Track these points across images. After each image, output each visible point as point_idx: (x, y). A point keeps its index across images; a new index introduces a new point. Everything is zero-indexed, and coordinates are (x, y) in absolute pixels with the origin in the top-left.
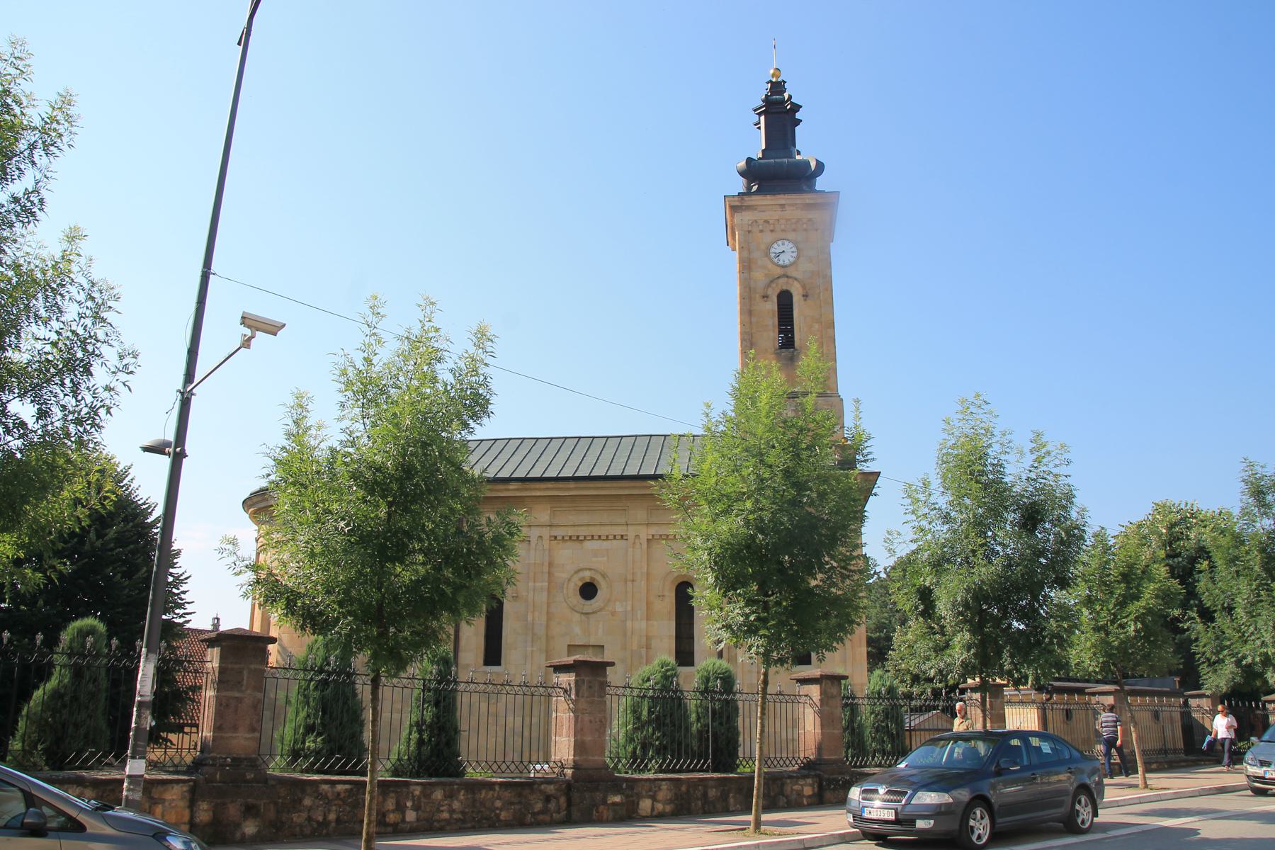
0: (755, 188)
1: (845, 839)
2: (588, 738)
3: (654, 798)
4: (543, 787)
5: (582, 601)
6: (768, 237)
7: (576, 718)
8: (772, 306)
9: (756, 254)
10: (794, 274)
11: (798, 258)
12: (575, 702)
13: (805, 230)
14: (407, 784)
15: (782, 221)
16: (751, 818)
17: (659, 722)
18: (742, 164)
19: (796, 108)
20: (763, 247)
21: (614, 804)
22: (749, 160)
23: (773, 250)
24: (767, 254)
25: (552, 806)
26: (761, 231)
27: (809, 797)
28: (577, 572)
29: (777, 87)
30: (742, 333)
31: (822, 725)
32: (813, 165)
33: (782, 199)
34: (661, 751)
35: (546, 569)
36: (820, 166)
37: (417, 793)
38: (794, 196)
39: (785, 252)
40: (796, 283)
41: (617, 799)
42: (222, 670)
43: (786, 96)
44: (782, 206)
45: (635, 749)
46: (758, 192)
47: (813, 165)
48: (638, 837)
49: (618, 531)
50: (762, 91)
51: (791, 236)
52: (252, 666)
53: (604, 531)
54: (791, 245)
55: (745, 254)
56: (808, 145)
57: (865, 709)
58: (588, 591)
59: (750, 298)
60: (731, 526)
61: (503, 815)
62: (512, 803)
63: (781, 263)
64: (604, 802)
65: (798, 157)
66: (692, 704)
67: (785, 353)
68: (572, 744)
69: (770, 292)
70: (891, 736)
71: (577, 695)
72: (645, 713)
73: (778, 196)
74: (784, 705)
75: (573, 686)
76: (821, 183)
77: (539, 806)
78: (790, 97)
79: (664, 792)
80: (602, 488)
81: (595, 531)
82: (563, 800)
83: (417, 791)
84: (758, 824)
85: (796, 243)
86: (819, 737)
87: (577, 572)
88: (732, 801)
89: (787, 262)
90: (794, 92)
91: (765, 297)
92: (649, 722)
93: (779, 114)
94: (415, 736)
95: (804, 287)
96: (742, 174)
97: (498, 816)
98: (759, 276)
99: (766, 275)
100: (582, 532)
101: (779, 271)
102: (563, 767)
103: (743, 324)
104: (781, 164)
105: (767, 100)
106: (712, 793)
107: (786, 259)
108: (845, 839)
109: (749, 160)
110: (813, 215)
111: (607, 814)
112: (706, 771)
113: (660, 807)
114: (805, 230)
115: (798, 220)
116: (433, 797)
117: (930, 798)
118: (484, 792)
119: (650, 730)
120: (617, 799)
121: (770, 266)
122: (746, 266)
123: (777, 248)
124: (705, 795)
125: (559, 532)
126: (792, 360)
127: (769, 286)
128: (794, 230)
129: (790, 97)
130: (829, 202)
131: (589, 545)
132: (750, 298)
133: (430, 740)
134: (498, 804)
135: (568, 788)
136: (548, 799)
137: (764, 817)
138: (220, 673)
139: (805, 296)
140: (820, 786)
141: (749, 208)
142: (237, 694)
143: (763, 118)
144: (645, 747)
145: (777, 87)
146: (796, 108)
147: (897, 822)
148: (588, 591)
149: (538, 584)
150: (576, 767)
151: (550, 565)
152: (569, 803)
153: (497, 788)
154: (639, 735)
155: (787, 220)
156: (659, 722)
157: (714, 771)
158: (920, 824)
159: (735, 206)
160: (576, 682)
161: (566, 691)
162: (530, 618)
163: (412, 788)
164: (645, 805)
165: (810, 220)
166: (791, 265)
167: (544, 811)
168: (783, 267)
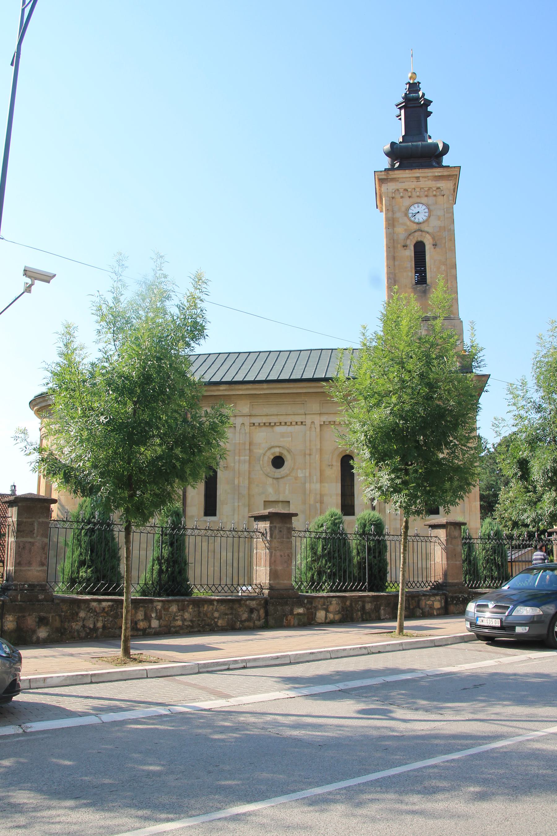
0: (397, 165)
1: (464, 640)
2: (279, 568)
3: (327, 610)
4: (248, 602)
5: (274, 469)
6: (406, 202)
7: (271, 553)
8: (410, 253)
9: (398, 215)
10: (426, 229)
11: (429, 216)
12: (270, 542)
13: (435, 196)
14: (151, 601)
15: (418, 190)
16: (396, 624)
17: (330, 556)
18: (387, 147)
19: (428, 103)
20: (403, 209)
21: (299, 614)
22: (393, 144)
23: (410, 211)
24: (406, 215)
25: (254, 616)
26: (402, 197)
27: (438, 609)
28: (270, 448)
29: (414, 87)
30: (388, 273)
31: (447, 558)
32: (441, 147)
33: (417, 173)
34: (332, 576)
35: (247, 447)
36: (446, 148)
37: (159, 607)
38: (426, 170)
39: (420, 212)
41: (301, 611)
42: (19, 523)
43: (420, 94)
44: (418, 178)
45: (313, 575)
46: (399, 168)
47: (441, 147)
48: (316, 637)
49: (299, 419)
50: (403, 90)
51: (424, 200)
52: (41, 520)
53: (289, 419)
54: (424, 207)
55: (390, 214)
56: (436, 132)
57: (478, 546)
58: (278, 462)
59: (394, 247)
60: (380, 415)
61: (220, 623)
62: (226, 614)
63: (417, 221)
64: (291, 612)
65: (430, 141)
66: (353, 543)
67: (420, 287)
68: (268, 572)
69: (408, 242)
70: (497, 566)
71: (271, 536)
72: (320, 549)
74: (419, 543)
75: (268, 530)
76: (446, 160)
77: (245, 616)
78: (423, 95)
79: (334, 606)
80: (287, 388)
81: (283, 419)
82: (262, 612)
83: (159, 606)
84: (401, 628)
85: (428, 206)
86: (445, 566)
87: (270, 448)
88: (382, 612)
89: (421, 220)
90: (426, 91)
91: (405, 246)
92: (323, 556)
93: (415, 108)
94: (156, 567)
95: (433, 238)
96: (388, 154)
97: (216, 623)
98: (400, 231)
99: (406, 230)
100: (273, 420)
101: (415, 227)
102: (262, 588)
103: (388, 267)
104: (417, 146)
105: (406, 98)
106: (368, 606)
107: (421, 218)
108: (464, 640)
109: (393, 144)
111: (294, 621)
112: (364, 591)
113: (331, 616)
114: (435, 196)
115: (429, 189)
116: (170, 610)
117: (526, 611)
118: (206, 607)
119: (324, 562)
120: (301, 611)
121: (408, 223)
122: (391, 223)
123: (413, 210)
124: (363, 607)
125: (256, 420)
126: (425, 293)
127: (408, 238)
128: (427, 196)
129: (423, 95)
131: (278, 429)
132: (394, 247)
133: (167, 570)
134: (216, 614)
135: (266, 603)
136: (251, 611)
137: (406, 624)
138: (18, 525)
139: (435, 245)
140: (446, 602)
141: (393, 180)
142: (30, 540)
143: (403, 111)
144: (320, 574)
145: (414, 87)
146: (428, 103)
147: (502, 628)
148: (278, 462)
149: (242, 458)
150: (271, 588)
151: (250, 444)
152: (267, 614)
153: (215, 603)
154: (316, 565)
156: (330, 556)
157: (369, 591)
158: (519, 630)
159: (383, 179)
160: (271, 528)
161: (263, 534)
162: (236, 482)
163: (155, 604)
164: (321, 615)
165: (438, 188)
167: (249, 619)
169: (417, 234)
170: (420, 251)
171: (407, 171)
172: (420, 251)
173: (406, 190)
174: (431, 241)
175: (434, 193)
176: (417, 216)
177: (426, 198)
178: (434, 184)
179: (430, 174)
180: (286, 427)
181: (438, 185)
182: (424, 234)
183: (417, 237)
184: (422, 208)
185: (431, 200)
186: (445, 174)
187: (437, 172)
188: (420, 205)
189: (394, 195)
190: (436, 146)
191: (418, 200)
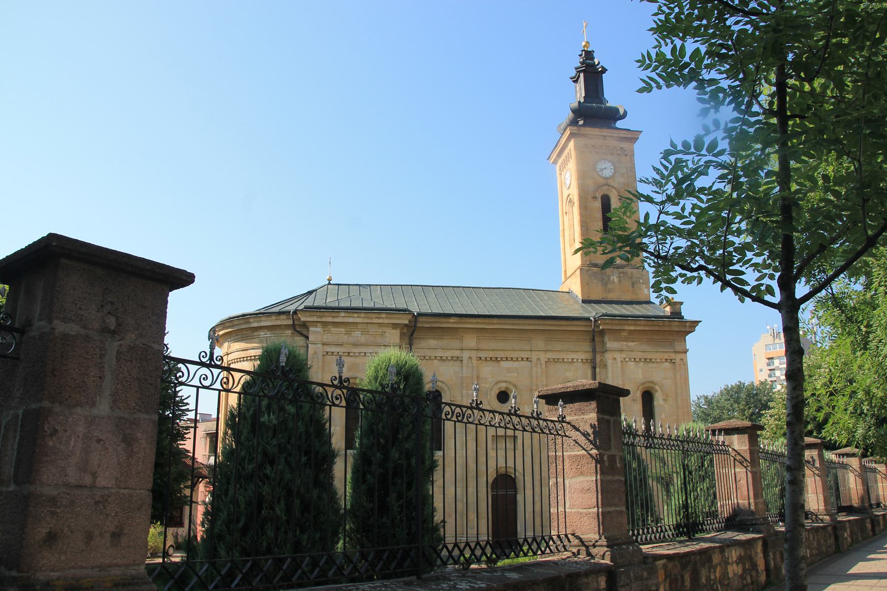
10: (613, 184)
11: (615, 173)
13: (619, 155)
32: (622, 112)
39: (607, 169)
81: (509, 354)
89: (608, 175)
91: (595, 198)
100: (500, 354)
101: (603, 181)
107: (608, 173)
114: (619, 155)
125: (483, 355)
128: (612, 154)
131: (504, 364)
168: (606, 178)
169: (605, 188)
176: (604, 171)
178: (615, 143)
181: (622, 146)
183: (604, 190)
184: (608, 165)
190: (617, 110)
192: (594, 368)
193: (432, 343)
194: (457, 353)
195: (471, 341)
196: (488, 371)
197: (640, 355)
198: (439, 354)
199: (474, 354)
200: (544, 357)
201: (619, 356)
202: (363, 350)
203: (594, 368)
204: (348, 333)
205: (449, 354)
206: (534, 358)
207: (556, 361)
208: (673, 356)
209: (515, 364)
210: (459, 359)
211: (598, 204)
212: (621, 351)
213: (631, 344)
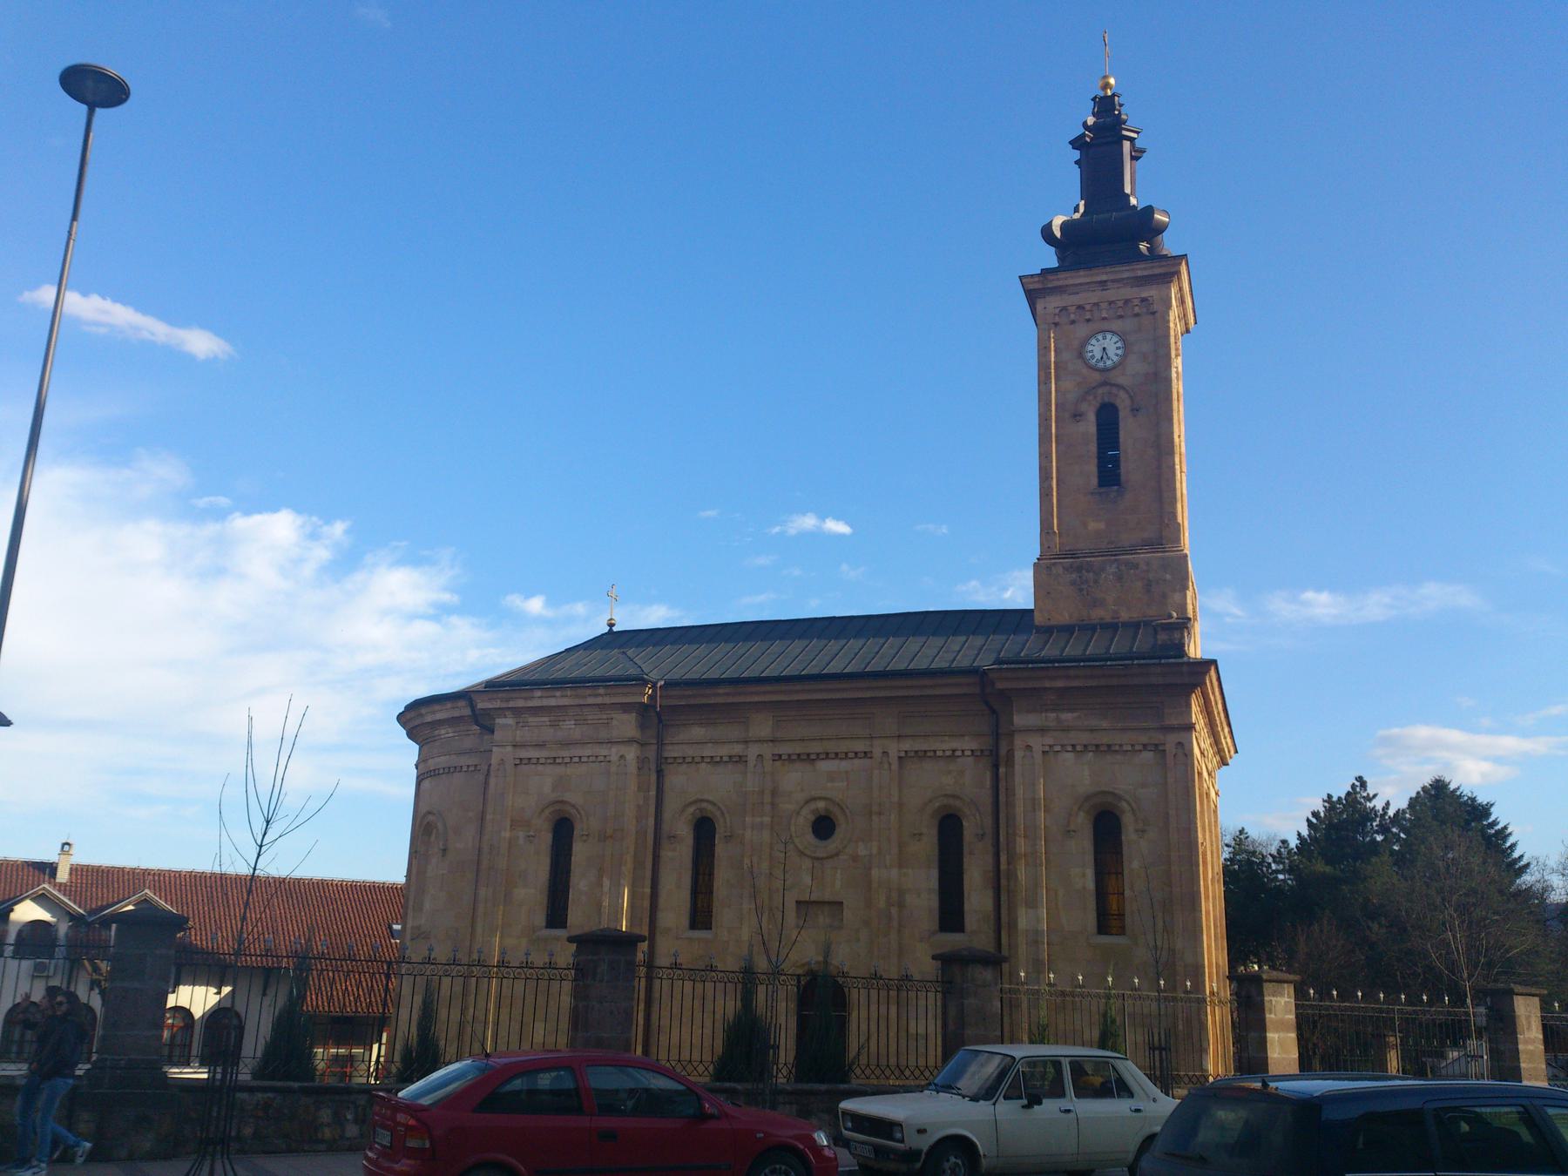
5: (810, 837)
6: (1082, 330)
10: (1121, 380)
11: (1124, 357)
13: (1137, 315)
15: (1104, 305)
26: (1073, 322)
28: (807, 802)
35: (767, 799)
39: (1105, 347)
40: (1122, 394)
49: (860, 746)
51: (1116, 325)
53: (844, 746)
54: (1115, 339)
58: (824, 826)
69: (1084, 407)
73: (1095, 271)
81: (832, 747)
85: (1122, 336)
87: (807, 802)
100: (815, 748)
101: (1097, 376)
110: (1150, 292)
115: (1127, 302)
121: (1085, 371)
125: (784, 749)
128: (1121, 317)
130: (1167, 269)
131: (824, 766)
141: (1060, 290)
148: (824, 826)
151: (774, 793)
155: (1111, 303)
165: (1144, 300)
166: (1114, 368)
168: (1105, 370)
169: (1106, 389)
170: (1108, 421)
171: (1082, 273)
172: (1108, 421)
173: (1080, 307)
174: (1128, 402)
175: (1137, 310)
177: (1120, 322)
178: (1128, 292)
179: (1126, 275)
180: (837, 762)
182: (1114, 390)
185: (1128, 324)
186: (1157, 271)
187: (1141, 270)
188: (1109, 336)
189: (1057, 319)
191: (1106, 325)
192: (996, 766)
193: (698, 732)
194: (737, 749)
195: (762, 726)
196: (793, 779)
197: (1085, 738)
198: (708, 751)
199: (767, 750)
200: (894, 749)
201: (1037, 742)
202: (577, 752)
203: (996, 766)
204: (554, 725)
205: (724, 751)
206: (877, 752)
207: (922, 755)
208: (1158, 737)
209: (845, 765)
210: (741, 760)
211: (1089, 426)
212: (1042, 730)
213: (1067, 716)
